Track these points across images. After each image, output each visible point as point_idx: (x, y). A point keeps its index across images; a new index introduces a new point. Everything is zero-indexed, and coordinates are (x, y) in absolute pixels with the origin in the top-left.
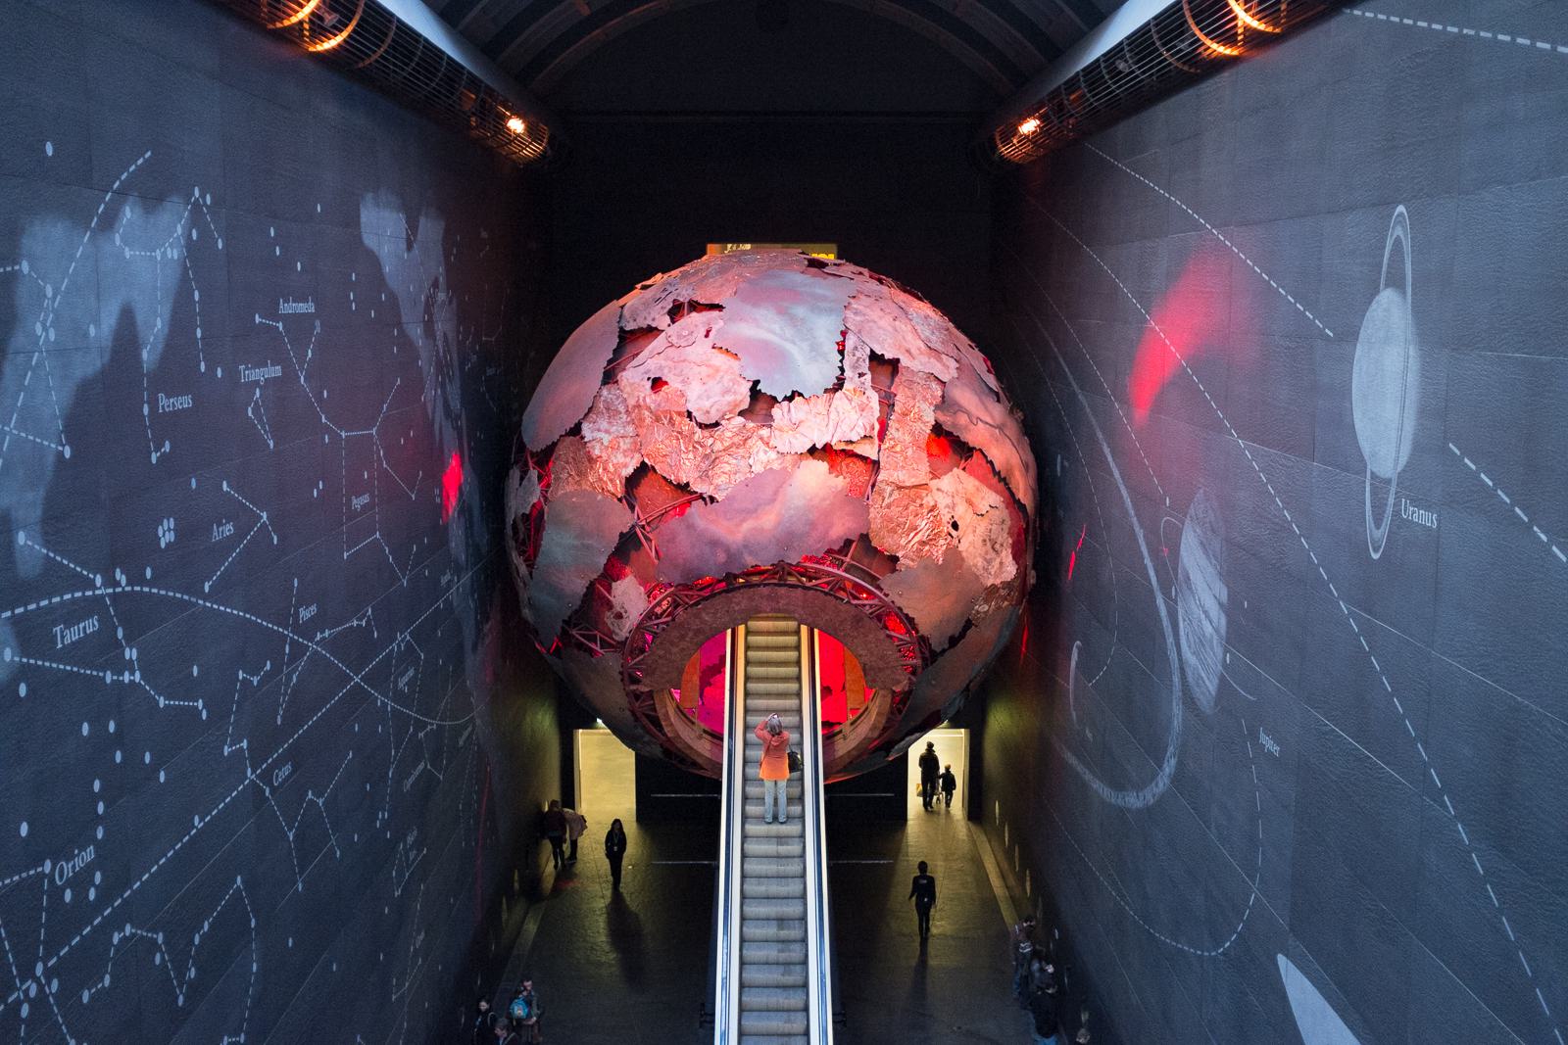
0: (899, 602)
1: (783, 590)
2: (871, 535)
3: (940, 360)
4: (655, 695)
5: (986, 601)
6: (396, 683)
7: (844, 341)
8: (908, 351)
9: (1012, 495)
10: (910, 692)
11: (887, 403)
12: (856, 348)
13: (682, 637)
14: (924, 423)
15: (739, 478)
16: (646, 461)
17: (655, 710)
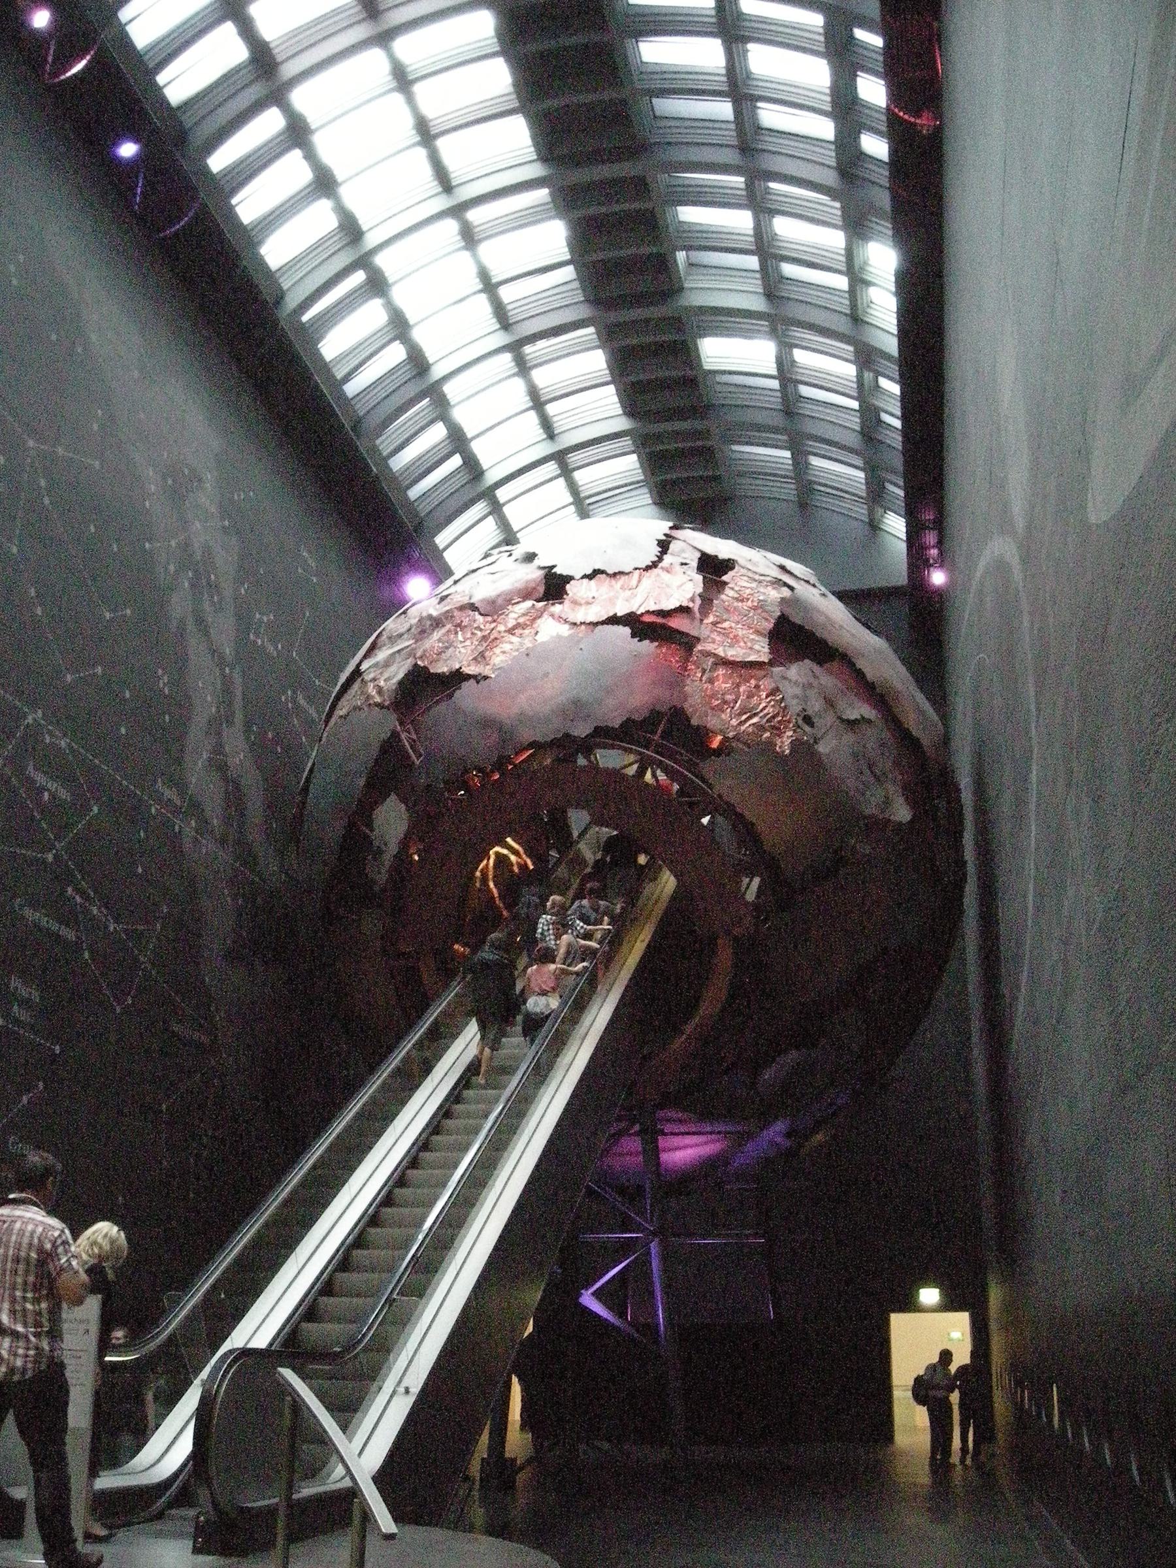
16: (419, 663)
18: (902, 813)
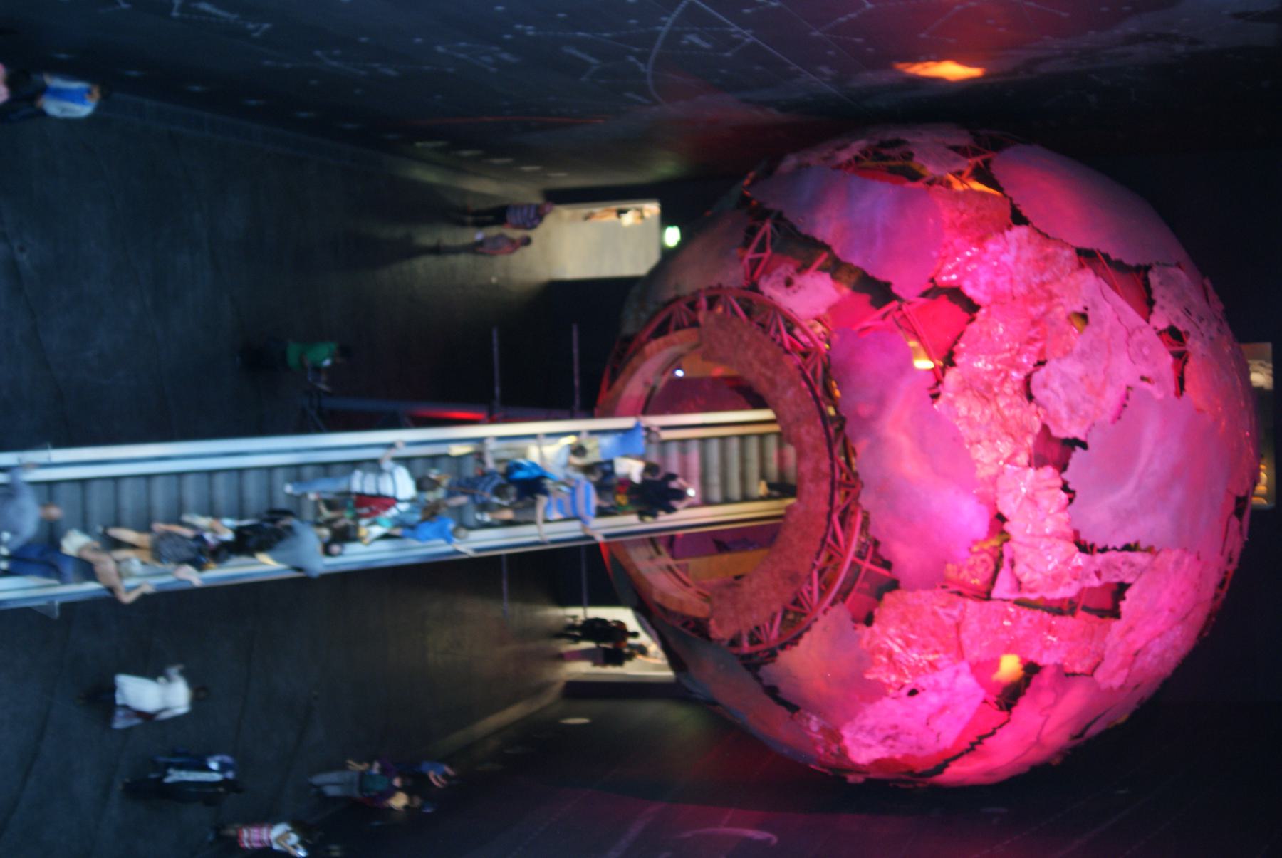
0: (817, 628)
1: (825, 486)
2: (897, 593)
3: (1121, 667)
4: (694, 330)
5: (823, 730)
6: (692, 32)
7: (1141, 550)
8: (1131, 629)
9: (955, 758)
10: (709, 639)
11: (1061, 609)
12: (1132, 565)
13: (765, 363)
14: (1041, 653)
15: (963, 428)
16: (983, 311)
17: (678, 328)
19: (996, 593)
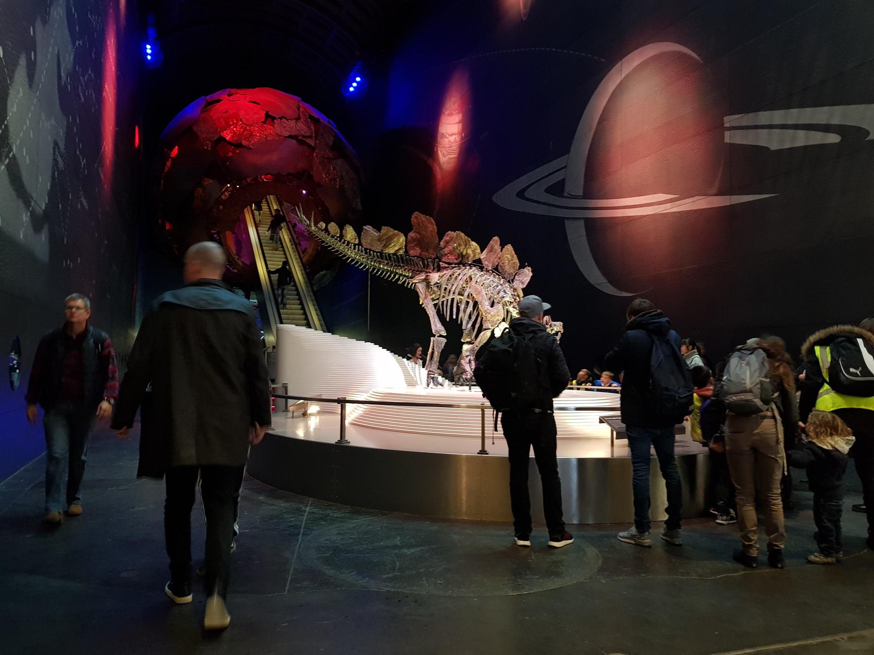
18: (359, 207)
19: (313, 145)
